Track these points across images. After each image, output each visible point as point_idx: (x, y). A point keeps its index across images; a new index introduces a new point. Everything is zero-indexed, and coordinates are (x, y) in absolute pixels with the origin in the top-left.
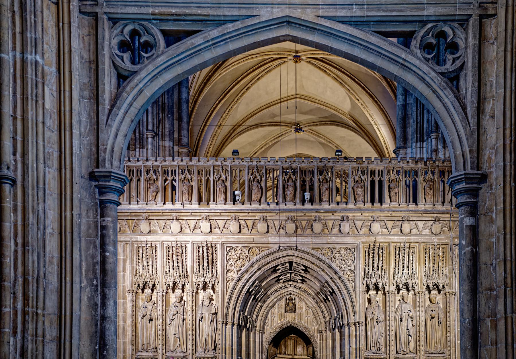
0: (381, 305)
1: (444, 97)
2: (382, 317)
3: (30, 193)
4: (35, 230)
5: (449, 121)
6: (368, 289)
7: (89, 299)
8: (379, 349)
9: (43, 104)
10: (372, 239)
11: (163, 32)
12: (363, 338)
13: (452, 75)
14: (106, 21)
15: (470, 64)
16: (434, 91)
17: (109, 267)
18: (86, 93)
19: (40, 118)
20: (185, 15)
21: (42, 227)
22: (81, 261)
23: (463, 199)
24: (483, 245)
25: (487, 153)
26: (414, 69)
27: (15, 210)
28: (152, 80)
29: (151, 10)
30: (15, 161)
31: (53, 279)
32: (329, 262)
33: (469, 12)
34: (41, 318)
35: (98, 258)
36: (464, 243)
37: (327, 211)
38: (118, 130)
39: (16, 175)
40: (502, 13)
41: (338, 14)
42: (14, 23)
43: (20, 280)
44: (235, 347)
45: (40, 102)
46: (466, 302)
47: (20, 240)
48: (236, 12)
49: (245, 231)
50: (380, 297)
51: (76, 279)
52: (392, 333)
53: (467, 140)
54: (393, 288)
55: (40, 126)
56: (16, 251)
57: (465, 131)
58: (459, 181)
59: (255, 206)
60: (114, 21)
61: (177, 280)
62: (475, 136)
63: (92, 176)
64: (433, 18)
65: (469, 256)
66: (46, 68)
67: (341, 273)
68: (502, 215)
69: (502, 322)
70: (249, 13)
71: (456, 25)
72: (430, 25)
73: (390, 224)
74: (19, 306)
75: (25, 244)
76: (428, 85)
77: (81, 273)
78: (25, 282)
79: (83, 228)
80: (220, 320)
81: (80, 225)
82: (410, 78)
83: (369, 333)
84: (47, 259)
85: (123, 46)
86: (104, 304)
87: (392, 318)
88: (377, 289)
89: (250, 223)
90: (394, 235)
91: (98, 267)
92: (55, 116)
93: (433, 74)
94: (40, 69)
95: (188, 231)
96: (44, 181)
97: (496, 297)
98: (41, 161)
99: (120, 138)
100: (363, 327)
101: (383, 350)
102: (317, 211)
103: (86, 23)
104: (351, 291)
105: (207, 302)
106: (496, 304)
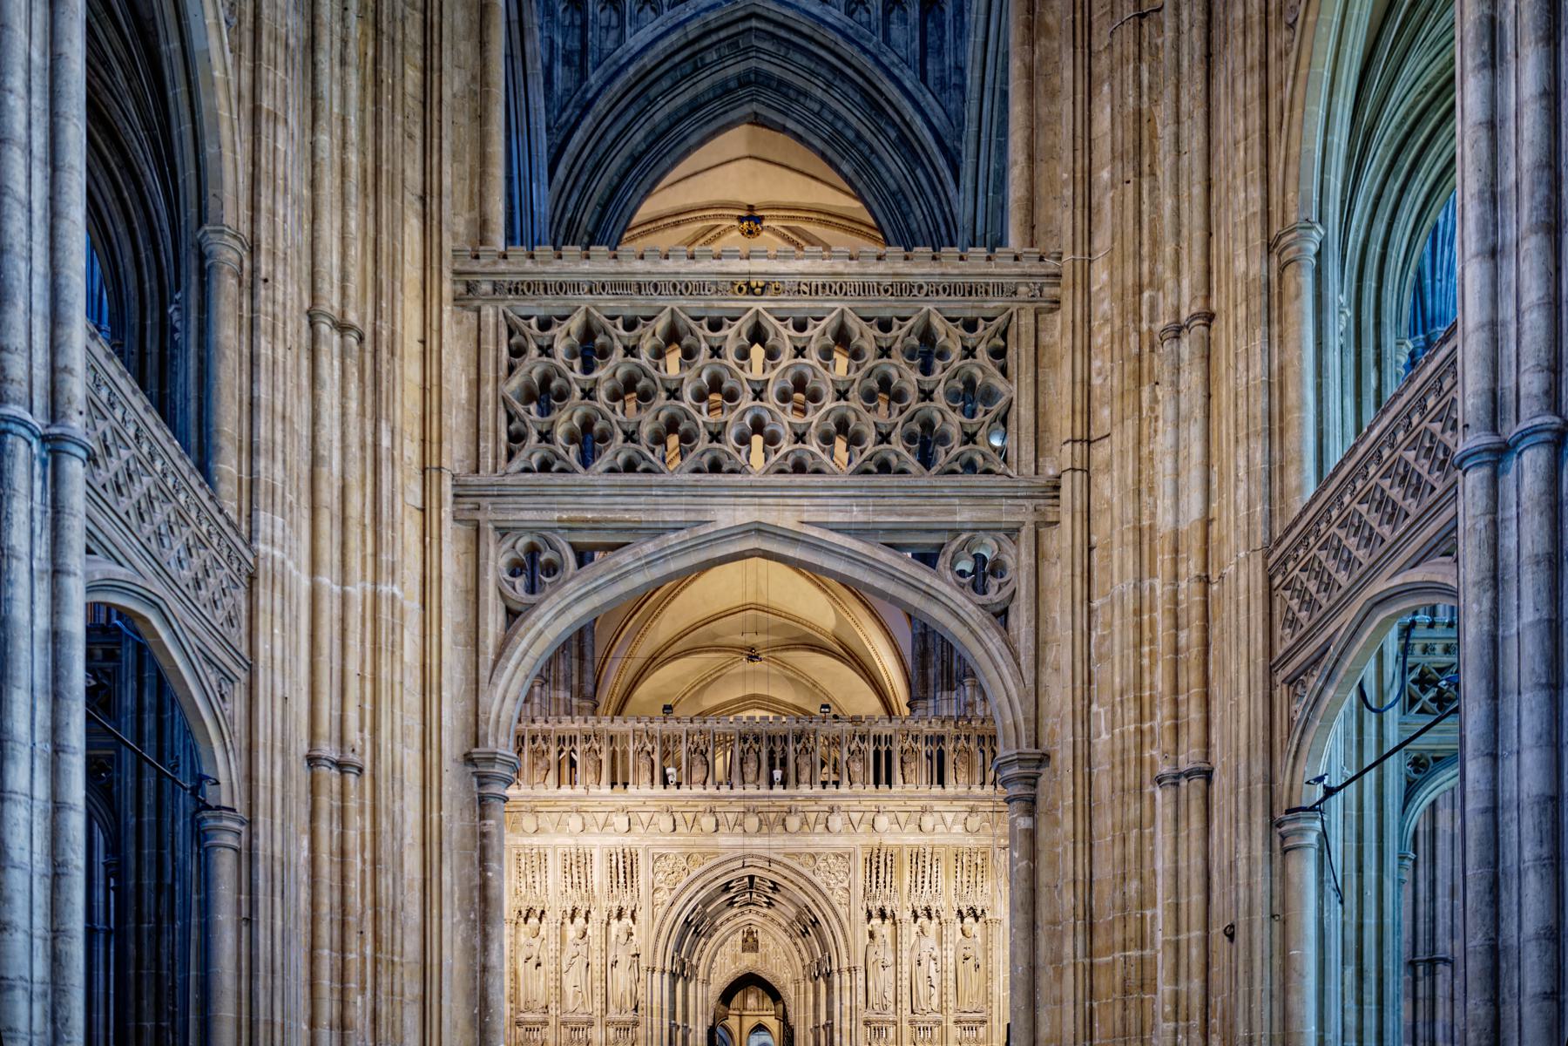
1: (987, 640)
3: (383, 786)
4: (390, 841)
5: (994, 675)
7: (464, 940)
9: (402, 656)
11: (573, 546)
13: (998, 609)
14: (491, 533)
15: (1023, 593)
16: (973, 632)
17: (492, 893)
18: (461, 637)
19: (397, 678)
20: (607, 521)
21: (398, 836)
22: (452, 885)
23: (1015, 790)
24: (1043, 859)
25: (1049, 723)
26: (943, 599)
27: (362, 812)
28: (556, 617)
29: (556, 515)
30: (363, 739)
31: (414, 912)
33: (1020, 518)
34: (398, 969)
35: (477, 881)
36: (1016, 855)
38: (506, 691)
39: (363, 761)
40: (1066, 520)
41: (831, 519)
42: (364, 542)
43: (369, 913)
45: (398, 653)
46: (1020, 942)
47: (368, 855)
48: (681, 517)
51: (446, 912)
53: (1021, 704)
55: (397, 687)
56: (363, 871)
57: (1018, 690)
58: (1009, 763)
60: (503, 532)
62: (1033, 698)
63: (468, 759)
64: (969, 526)
65: (1023, 874)
66: (406, 603)
68: (1071, 815)
69: (1070, 971)
70: (701, 519)
71: (1001, 535)
72: (964, 536)
74: (369, 950)
75: (375, 862)
76: (964, 623)
77: (452, 902)
78: (376, 916)
79: (455, 836)
81: (451, 832)
82: (937, 613)
84: (405, 882)
85: (515, 569)
86: (485, 949)
91: (476, 894)
92: (418, 673)
93: (971, 606)
94: (398, 605)
96: (402, 768)
97: (1062, 935)
98: (398, 739)
99: (508, 702)
103: (462, 534)
106: (1061, 945)
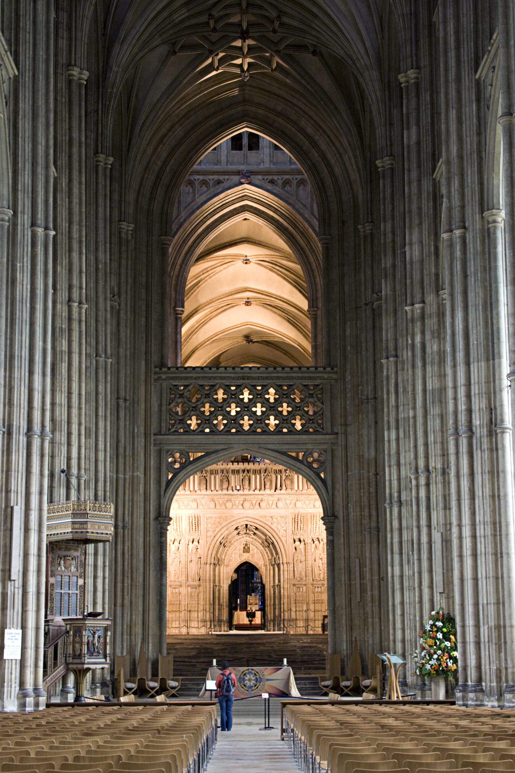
0: (303, 551)
2: (303, 559)
6: (295, 542)
8: (301, 579)
10: (296, 511)
12: (292, 572)
32: (270, 525)
37: (269, 495)
44: (212, 578)
49: (218, 507)
50: (302, 546)
52: (310, 569)
54: (310, 541)
59: (225, 492)
61: (176, 537)
67: (278, 532)
73: (307, 502)
80: (203, 562)
83: (295, 569)
87: (309, 559)
88: (300, 541)
89: (221, 502)
90: (310, 508)
95: (183, 507)
100: (292, 565)
101: (304, 579)
102: (263, 495)
104: (284, 543)
105: (194, 550)
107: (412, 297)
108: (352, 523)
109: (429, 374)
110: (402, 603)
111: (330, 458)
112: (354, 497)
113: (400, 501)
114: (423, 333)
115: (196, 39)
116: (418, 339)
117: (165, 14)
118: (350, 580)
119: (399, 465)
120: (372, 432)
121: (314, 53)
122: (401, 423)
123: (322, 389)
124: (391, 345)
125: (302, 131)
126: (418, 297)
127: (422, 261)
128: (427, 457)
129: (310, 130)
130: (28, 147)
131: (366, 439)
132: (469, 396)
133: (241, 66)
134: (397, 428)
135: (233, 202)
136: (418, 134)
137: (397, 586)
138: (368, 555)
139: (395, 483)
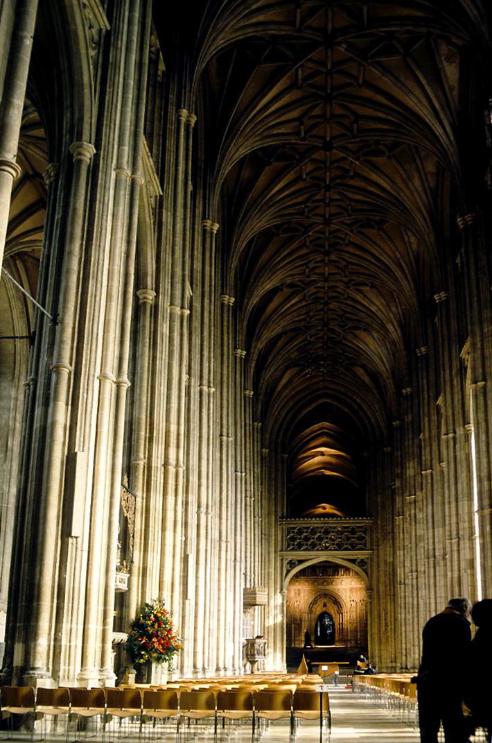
107: (410, 492)
108: (381, 594)
109: (418, 528)
110: (405, 631)
111: (369, 562)
112: (382, 580)
113: (405, 584)
114: (415, 509)
115: (302, 362)
116: (413, 512)
117: (287, 355)
118: (380, 620)
119: (404, 567)
120: (392, 548)
121: (361, 366)
122: (405, 547)
123: (365, 528)
124: (401, 510)
125: (355, 402)
126: (413, 493)
127: (415, 476)
128: (417, 565)
129: (358, 401)
130: (248, 454)
131: (388, 553)
132: (434, 543)
133: (323, 372)
134: (404, 549)
135: (317, 431)
136: (412, 417)
137: (403, 623)
138: (389, 608)
139: (403, 576)
